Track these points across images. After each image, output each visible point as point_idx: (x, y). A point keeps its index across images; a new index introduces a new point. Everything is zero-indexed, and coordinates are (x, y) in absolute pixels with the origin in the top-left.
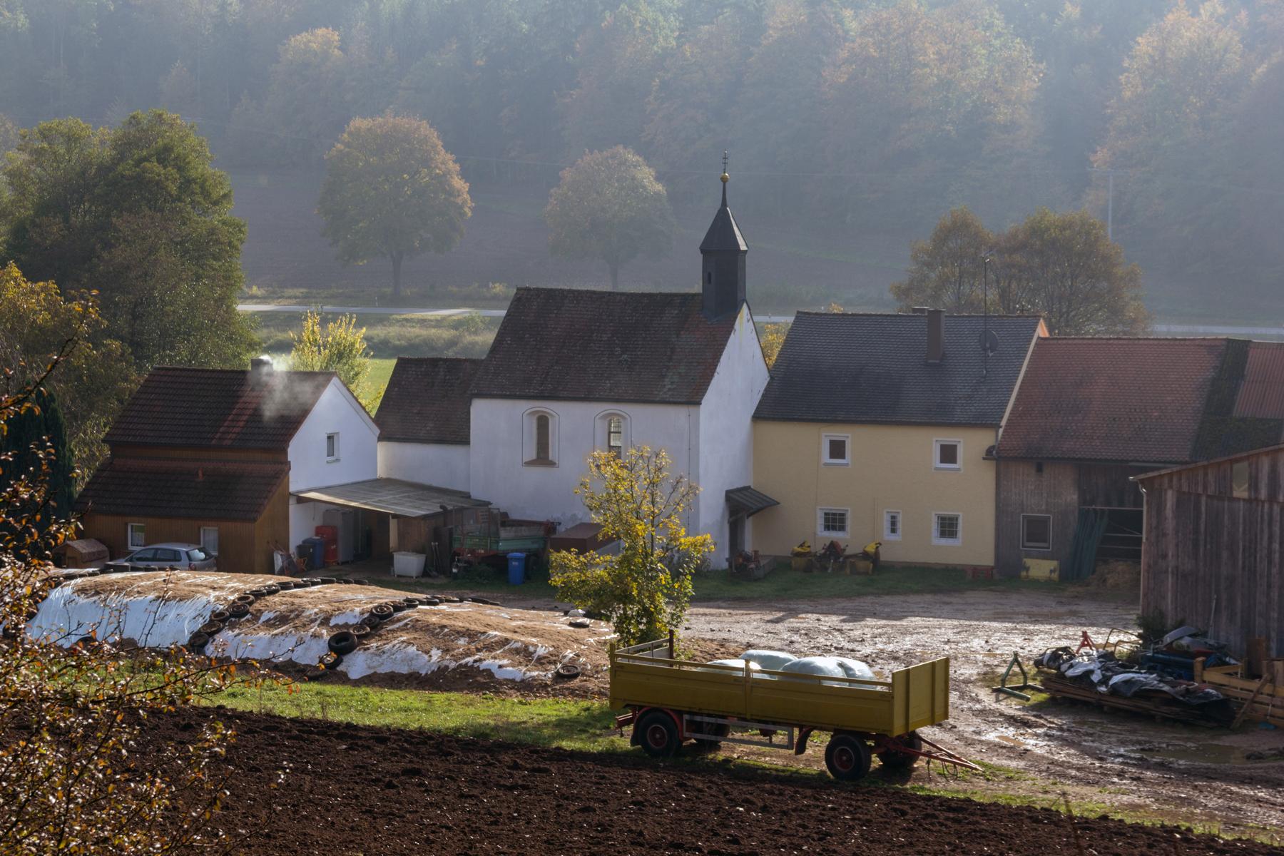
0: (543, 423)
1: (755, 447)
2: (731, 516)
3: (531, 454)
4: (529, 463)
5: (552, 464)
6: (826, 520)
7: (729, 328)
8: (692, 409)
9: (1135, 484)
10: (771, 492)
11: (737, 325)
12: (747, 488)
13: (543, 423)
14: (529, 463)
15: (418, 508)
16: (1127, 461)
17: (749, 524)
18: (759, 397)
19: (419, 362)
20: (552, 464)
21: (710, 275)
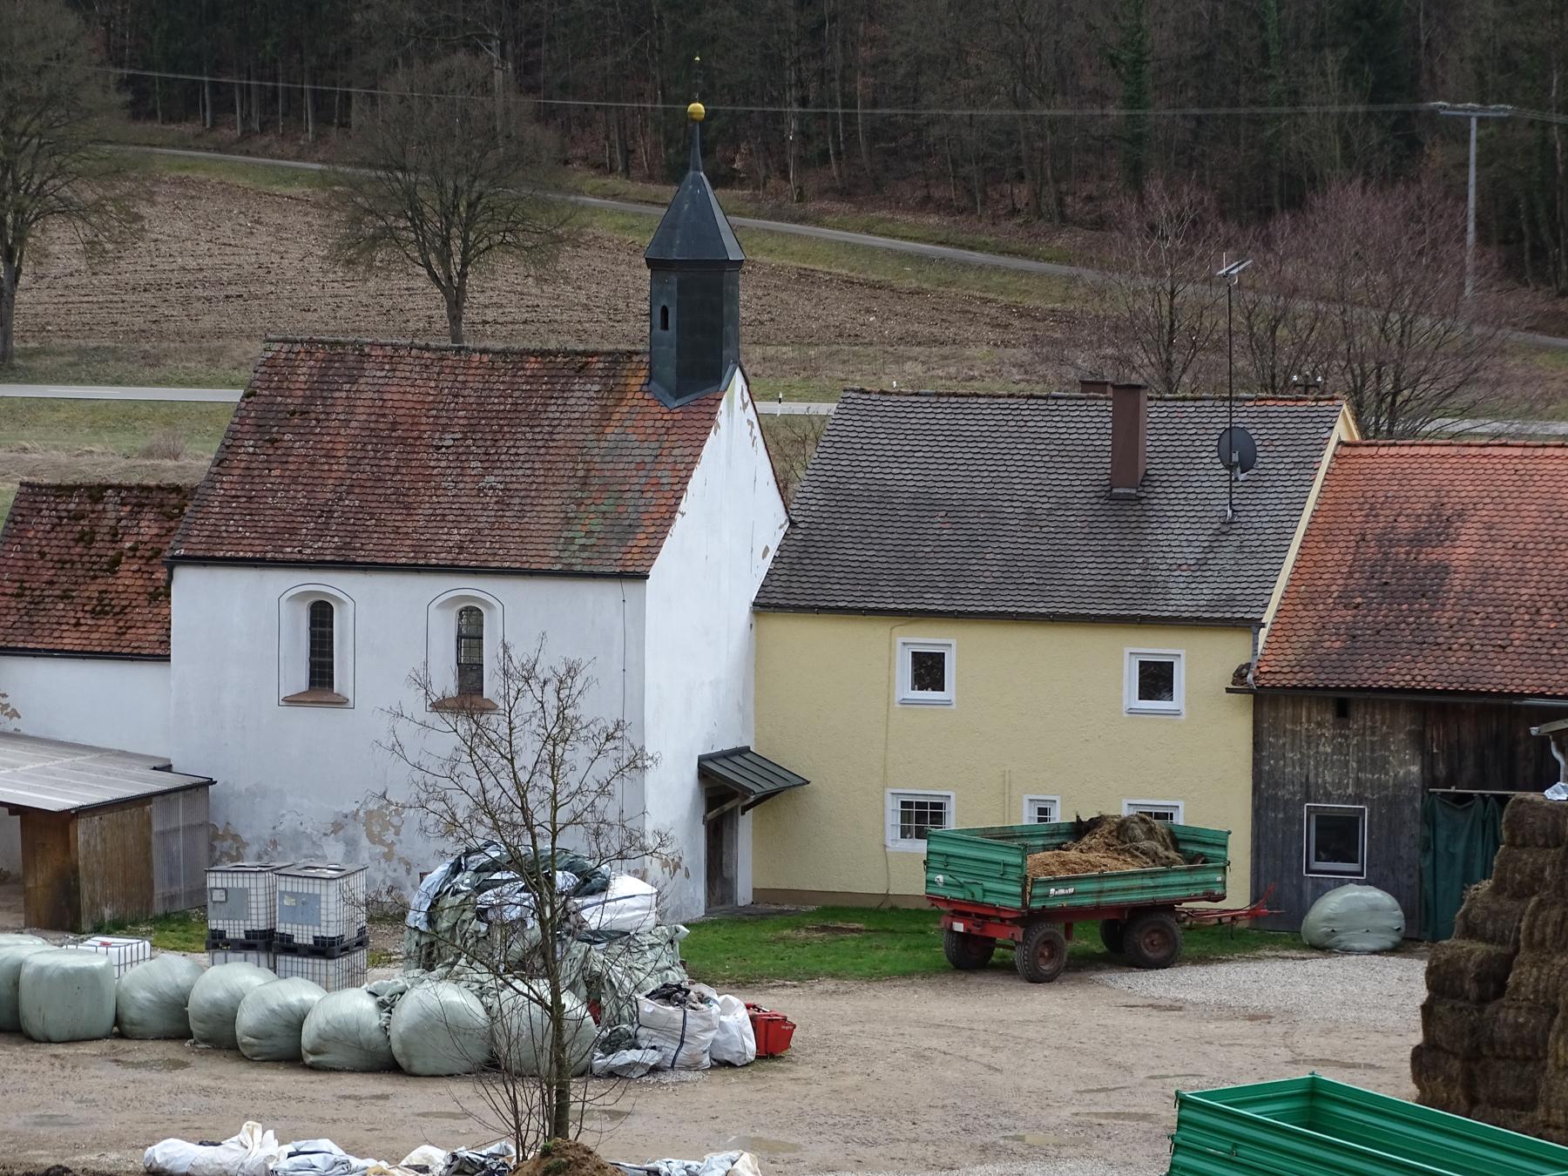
0: (321, 615)
1: (760, 665)
2: (709, 809)
3: (299, 679)
4: (292, 701)
5: (341, 702)
6: (905, 817)
7: (707, 422)
8: (629, 588)
9: (1543, 742)
10: (793, 759)
11: (722, 418)
12: (743, 751)
13: (321, 615)
14: (292, 701)
15: (68, 795)
16: (1522, 695)
17: (746, 825)
18: (767, 563)
19: (63, 490)
20: (341, 702)
21: (665, 311)
